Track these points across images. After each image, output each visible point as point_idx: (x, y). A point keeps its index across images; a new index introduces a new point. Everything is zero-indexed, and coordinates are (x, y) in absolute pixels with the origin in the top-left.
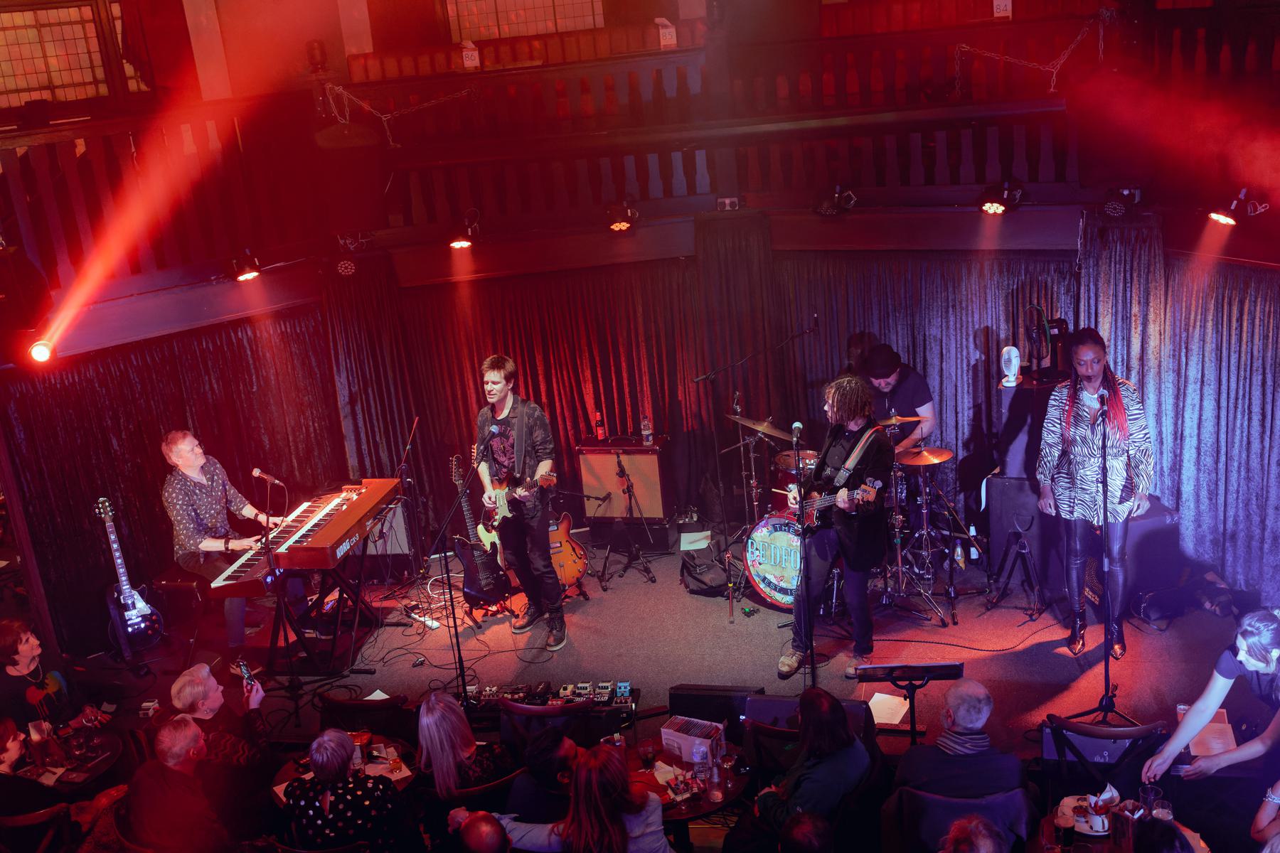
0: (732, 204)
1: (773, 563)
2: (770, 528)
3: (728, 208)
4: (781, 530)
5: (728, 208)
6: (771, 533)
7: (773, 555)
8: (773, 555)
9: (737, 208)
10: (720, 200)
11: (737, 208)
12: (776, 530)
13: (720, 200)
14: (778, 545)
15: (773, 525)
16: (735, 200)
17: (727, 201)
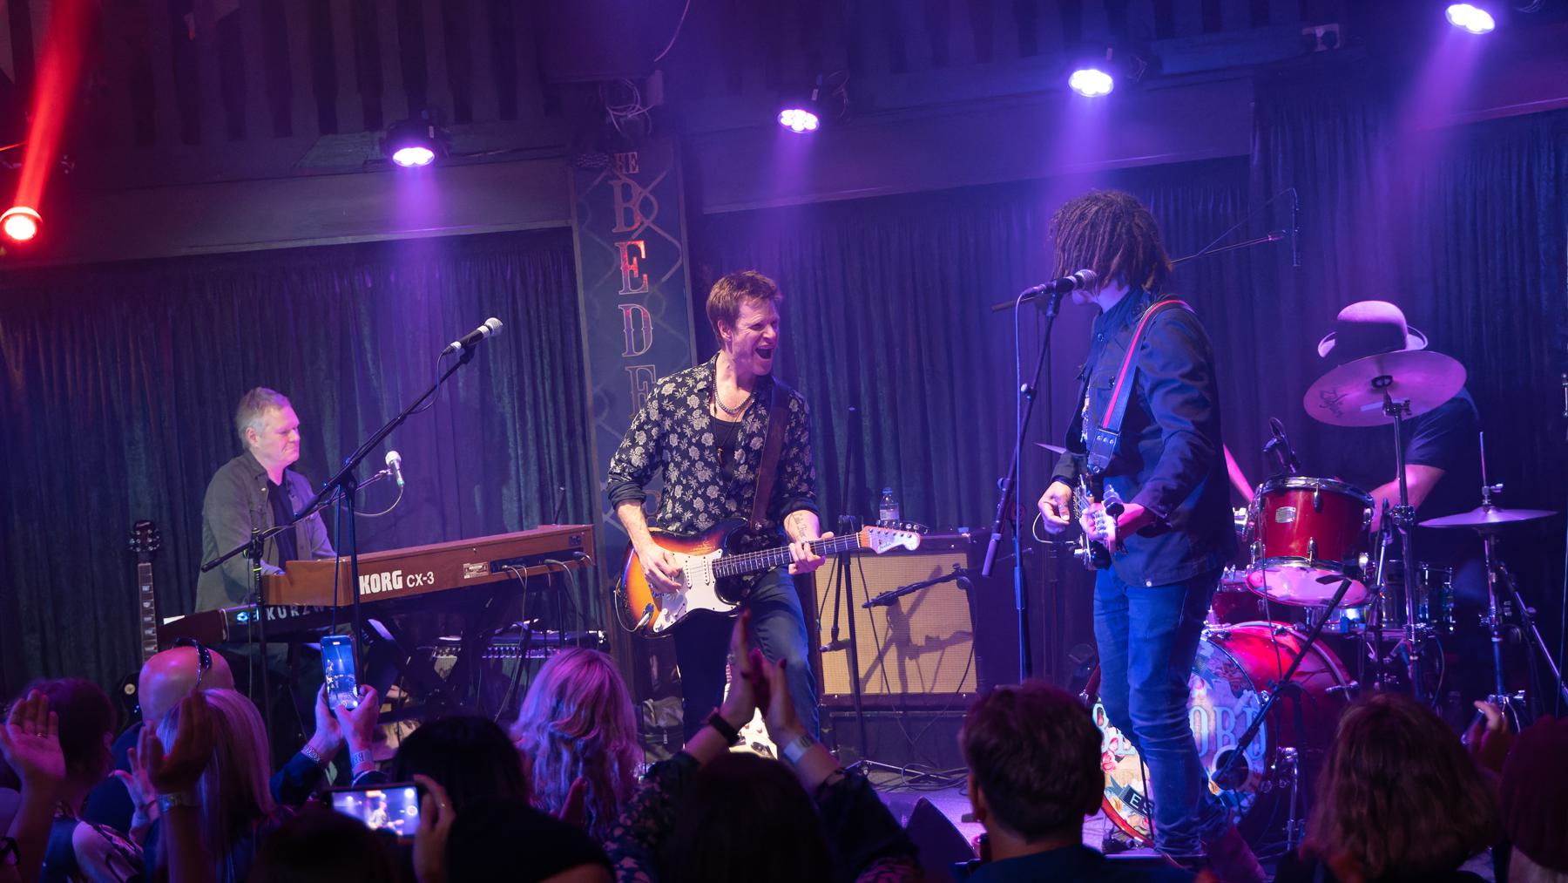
0: (1329, 36)
5: (1321, 48)
10: (1306, 31)
11: (1338, 45)
13: (1306, 31)
16: (1335, 27)
17: (1320, 31)
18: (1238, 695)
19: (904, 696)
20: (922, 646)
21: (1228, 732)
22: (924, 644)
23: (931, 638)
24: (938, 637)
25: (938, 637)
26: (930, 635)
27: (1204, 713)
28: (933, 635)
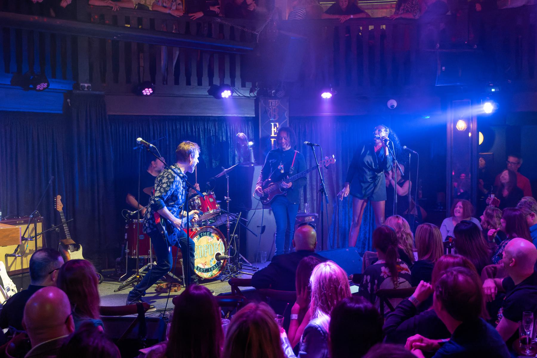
0: (88, 87)
1: (201, 257)
2: (198, 236)
3: (86, 89)
4: (203, 236)
5: (86, 89)
6: (198, 239)
7: (200, 252)
8: (200, 252)
9: (90, 90)
10: (81, 84)
11: (90, 90)
12: (201, 237)
14: (202, 245)
15: (199, 234)
16: (90, 85)
17: (86, 85)
18: (218, 240)
19: (23, 270)
20: (28, 253)
21: (217, 249)
22: (29, 252)
23: (31, 250)
24: (33, 249)
25: (33, 249)
26: (30, 249)
27: (212, 245)
28: (32, 249)
